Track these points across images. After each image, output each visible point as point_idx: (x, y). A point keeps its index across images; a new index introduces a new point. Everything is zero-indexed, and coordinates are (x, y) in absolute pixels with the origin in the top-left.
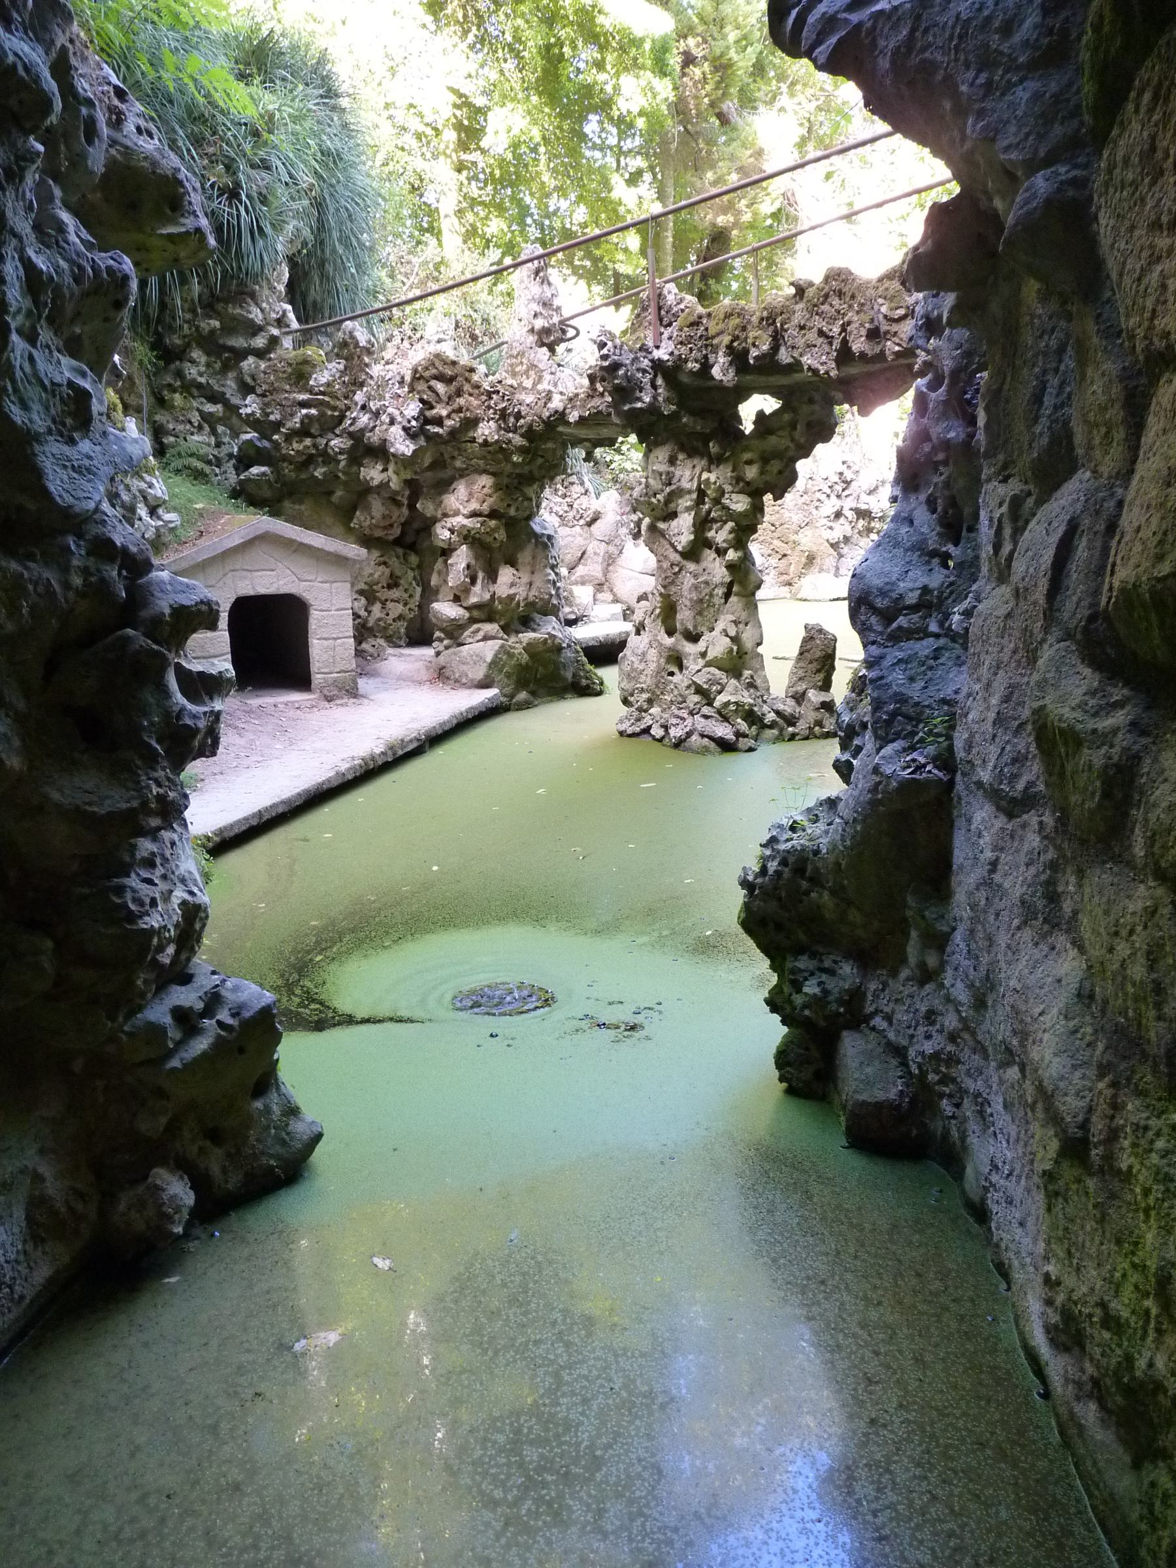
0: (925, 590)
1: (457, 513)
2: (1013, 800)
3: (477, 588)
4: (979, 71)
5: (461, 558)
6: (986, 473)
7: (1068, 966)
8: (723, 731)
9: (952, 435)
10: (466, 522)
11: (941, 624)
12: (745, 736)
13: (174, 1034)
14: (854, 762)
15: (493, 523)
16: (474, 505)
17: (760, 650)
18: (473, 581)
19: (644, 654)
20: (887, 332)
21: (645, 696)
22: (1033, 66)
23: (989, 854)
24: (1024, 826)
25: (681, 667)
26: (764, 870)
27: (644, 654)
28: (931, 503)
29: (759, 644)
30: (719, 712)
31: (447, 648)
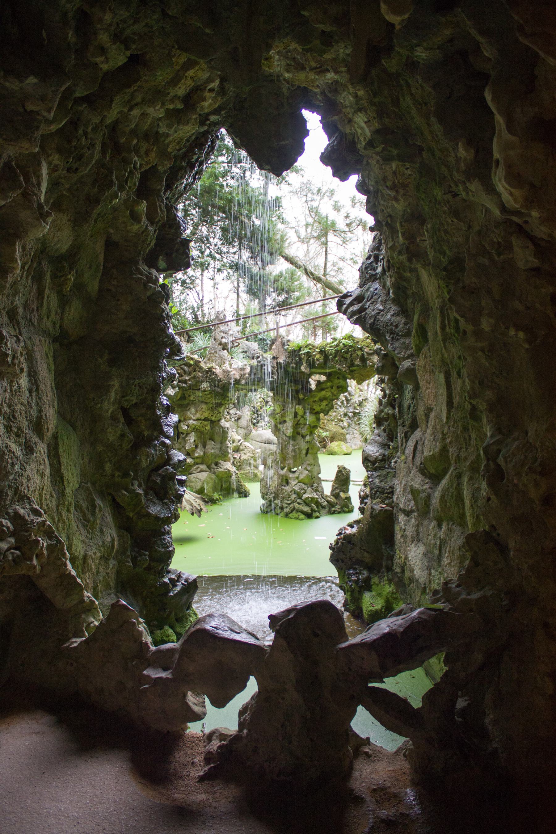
0: (384, 455)
1: (190, 419)
3: (198, 450)
4: (391, 334)
5: (192, 438)
6: (399, 423)
7: (421, 549)
8: (306, 509)
9: (390, 412)
10: (194, 422)
11: (389, 465)
12: (315, 511)
13: (171, 586)
15: (206, 423)
16: (198, 416)
17: (320, 476)
18: (197, 447)
20: (367, 358)
23: (403, 528)
24: (411, 518)
25: (288, 483)
29: (319, 473)
30: (304, 502)
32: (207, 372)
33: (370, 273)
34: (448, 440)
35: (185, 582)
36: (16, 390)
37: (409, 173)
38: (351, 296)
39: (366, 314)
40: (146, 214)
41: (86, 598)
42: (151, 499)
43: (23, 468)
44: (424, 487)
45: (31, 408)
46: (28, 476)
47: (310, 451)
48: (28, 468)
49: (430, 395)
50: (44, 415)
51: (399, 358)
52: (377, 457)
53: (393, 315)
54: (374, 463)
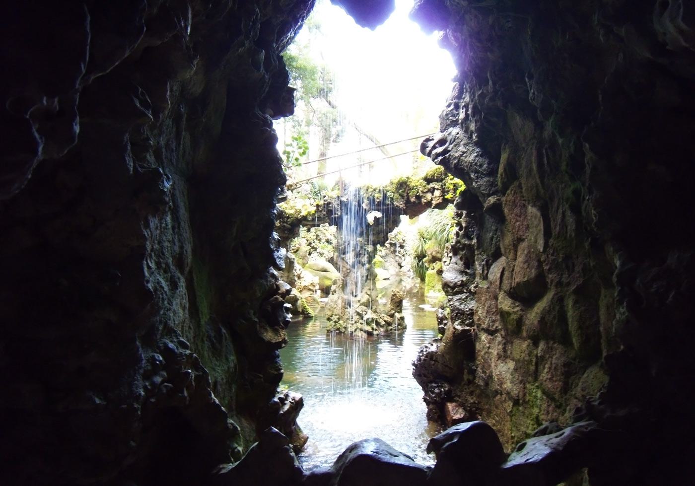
0: (462, 281)
2: (493, 331)
7: (511, 365)
9: (466, 242)
13: (281, 405)
14: (445, 327)
19: (336, 302)
20: (422, 196)
21: (337, 317)
22: (486, 175)
23: (488, 345)
24: (496, 337)
26: (419, 360)
27: (336, 302)
28: (461, 259)
33: (451, 119)
34: (546, 268)
35: (292, 400)
36: (164, 227)
37: (510, 25)
38: (433, 140)
39: (450, 155)
40: (264, 63)
41: (230, 425)
43: (170, 303)
44: (516, 310)
45: (175, 244)
46: (174, 310)
48: (174, 303)
49: (521, 227)
50: (185, 251)
51: (483, 194)
52: (456, 283)
53: (476, 156)
54: (453, 288)
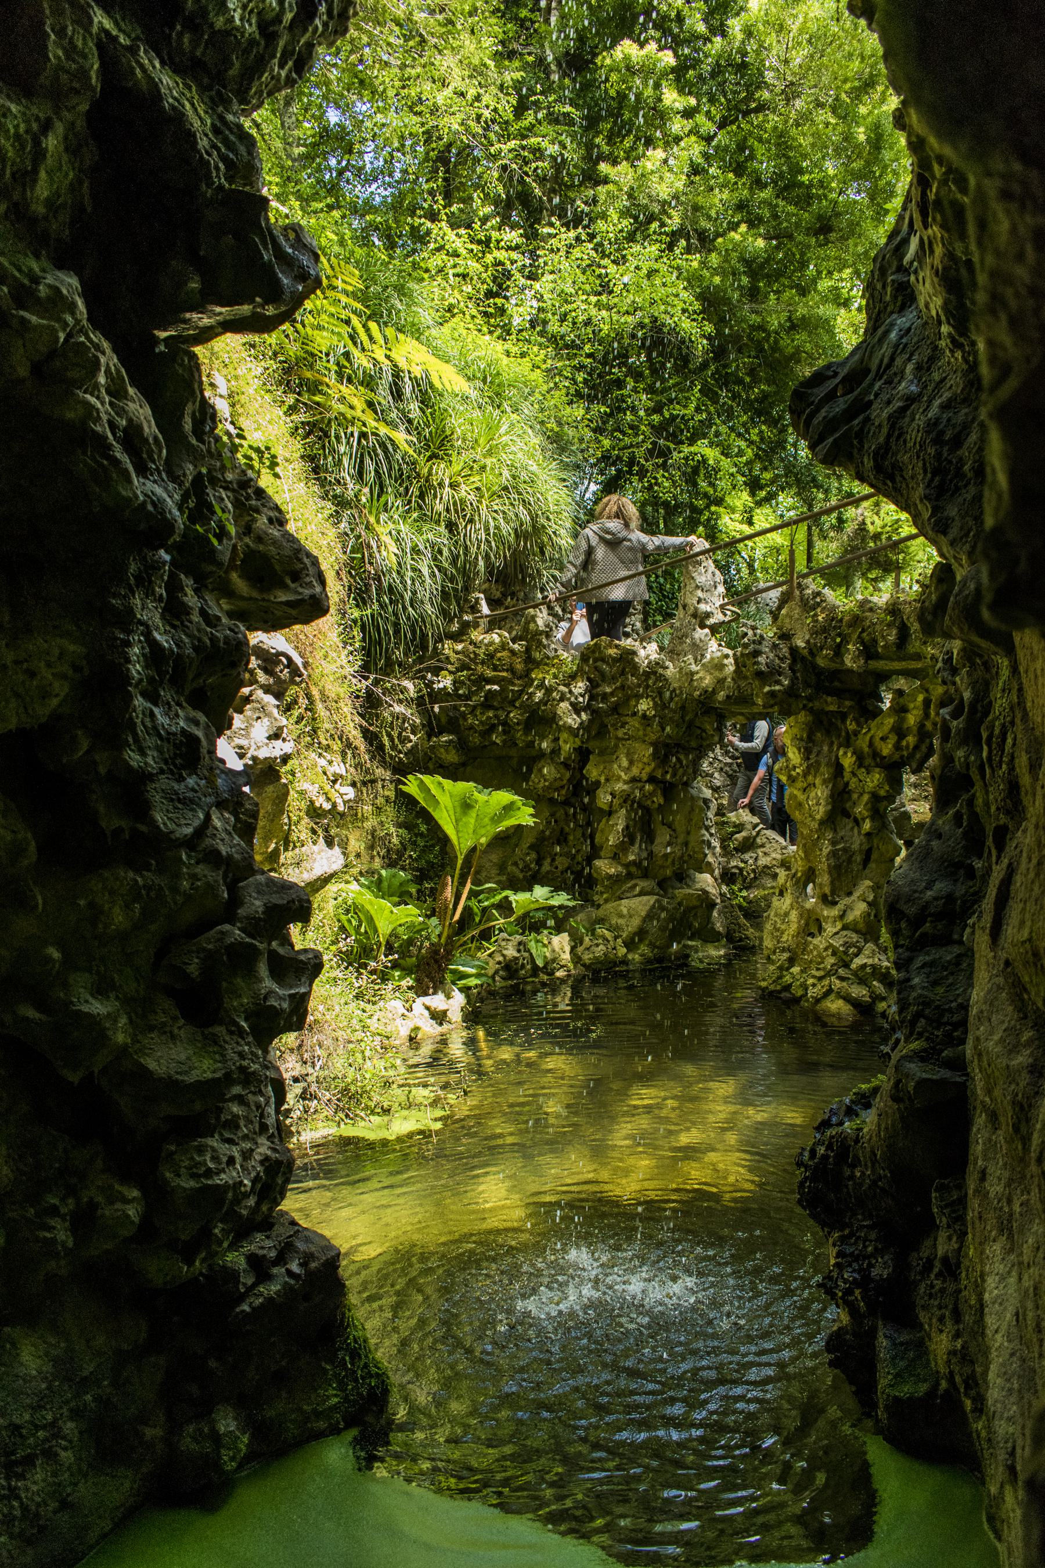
3: (636, 848)
16: (635, 771)
31: (606, 901)
32: (647, 675)
42: (164, 1024)
47: (874, 856)
